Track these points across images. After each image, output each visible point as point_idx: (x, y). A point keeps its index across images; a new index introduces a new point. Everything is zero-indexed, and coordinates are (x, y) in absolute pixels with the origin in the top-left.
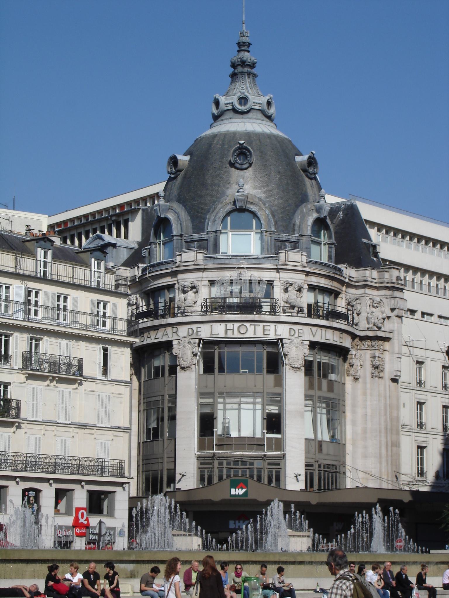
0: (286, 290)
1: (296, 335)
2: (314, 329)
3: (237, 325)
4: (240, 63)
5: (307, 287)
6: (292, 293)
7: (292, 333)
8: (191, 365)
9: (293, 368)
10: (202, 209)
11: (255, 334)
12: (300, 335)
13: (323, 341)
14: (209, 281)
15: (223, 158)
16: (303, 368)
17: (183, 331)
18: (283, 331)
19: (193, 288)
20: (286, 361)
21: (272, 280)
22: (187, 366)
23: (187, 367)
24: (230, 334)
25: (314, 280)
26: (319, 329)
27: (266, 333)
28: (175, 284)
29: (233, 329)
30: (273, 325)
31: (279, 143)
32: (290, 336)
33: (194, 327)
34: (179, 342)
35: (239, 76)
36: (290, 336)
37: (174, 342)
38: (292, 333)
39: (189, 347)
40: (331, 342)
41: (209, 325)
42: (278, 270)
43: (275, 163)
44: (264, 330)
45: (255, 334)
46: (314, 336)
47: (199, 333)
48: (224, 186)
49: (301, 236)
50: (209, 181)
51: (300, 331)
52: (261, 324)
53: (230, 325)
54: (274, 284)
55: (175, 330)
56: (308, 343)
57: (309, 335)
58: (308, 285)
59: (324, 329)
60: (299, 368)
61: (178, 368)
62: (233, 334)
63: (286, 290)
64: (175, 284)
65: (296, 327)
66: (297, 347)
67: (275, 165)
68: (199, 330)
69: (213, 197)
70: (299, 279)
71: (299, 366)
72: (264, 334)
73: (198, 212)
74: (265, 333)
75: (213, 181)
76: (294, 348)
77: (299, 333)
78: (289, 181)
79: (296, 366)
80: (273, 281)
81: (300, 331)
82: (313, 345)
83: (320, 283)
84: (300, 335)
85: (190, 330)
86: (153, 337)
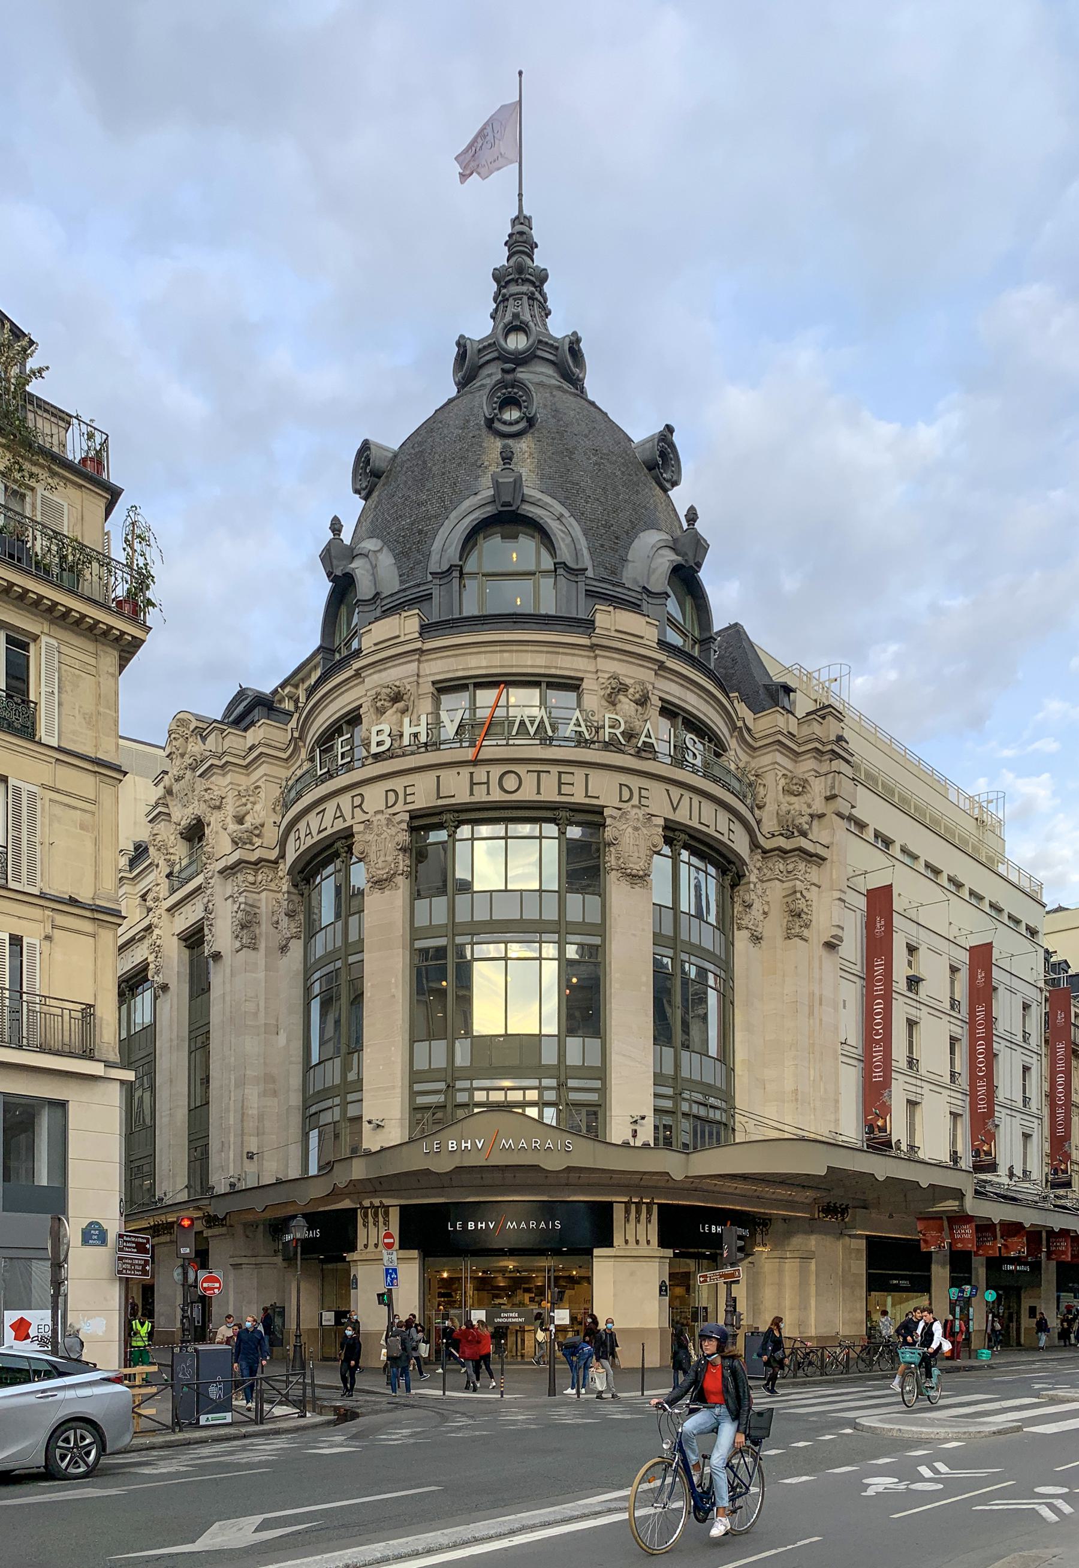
1: (635, 801)
6: (626, 705)
7: (626, 795)
12: (644, 801)
17: (374, 797)
19: (397, 698)
20: (611, 860)
21: (580, 675)
32: (621, 801)
33: (397, 784)
36: (621, 801)
38: (626, 797)
47: (409, 799)
54: (584, 685)
65: (635, 782)
66: (636, 829)
76: (630, 830)
77: (640, 797)
80: (582, 679)
84: (644, 801)
85: (391, 795)
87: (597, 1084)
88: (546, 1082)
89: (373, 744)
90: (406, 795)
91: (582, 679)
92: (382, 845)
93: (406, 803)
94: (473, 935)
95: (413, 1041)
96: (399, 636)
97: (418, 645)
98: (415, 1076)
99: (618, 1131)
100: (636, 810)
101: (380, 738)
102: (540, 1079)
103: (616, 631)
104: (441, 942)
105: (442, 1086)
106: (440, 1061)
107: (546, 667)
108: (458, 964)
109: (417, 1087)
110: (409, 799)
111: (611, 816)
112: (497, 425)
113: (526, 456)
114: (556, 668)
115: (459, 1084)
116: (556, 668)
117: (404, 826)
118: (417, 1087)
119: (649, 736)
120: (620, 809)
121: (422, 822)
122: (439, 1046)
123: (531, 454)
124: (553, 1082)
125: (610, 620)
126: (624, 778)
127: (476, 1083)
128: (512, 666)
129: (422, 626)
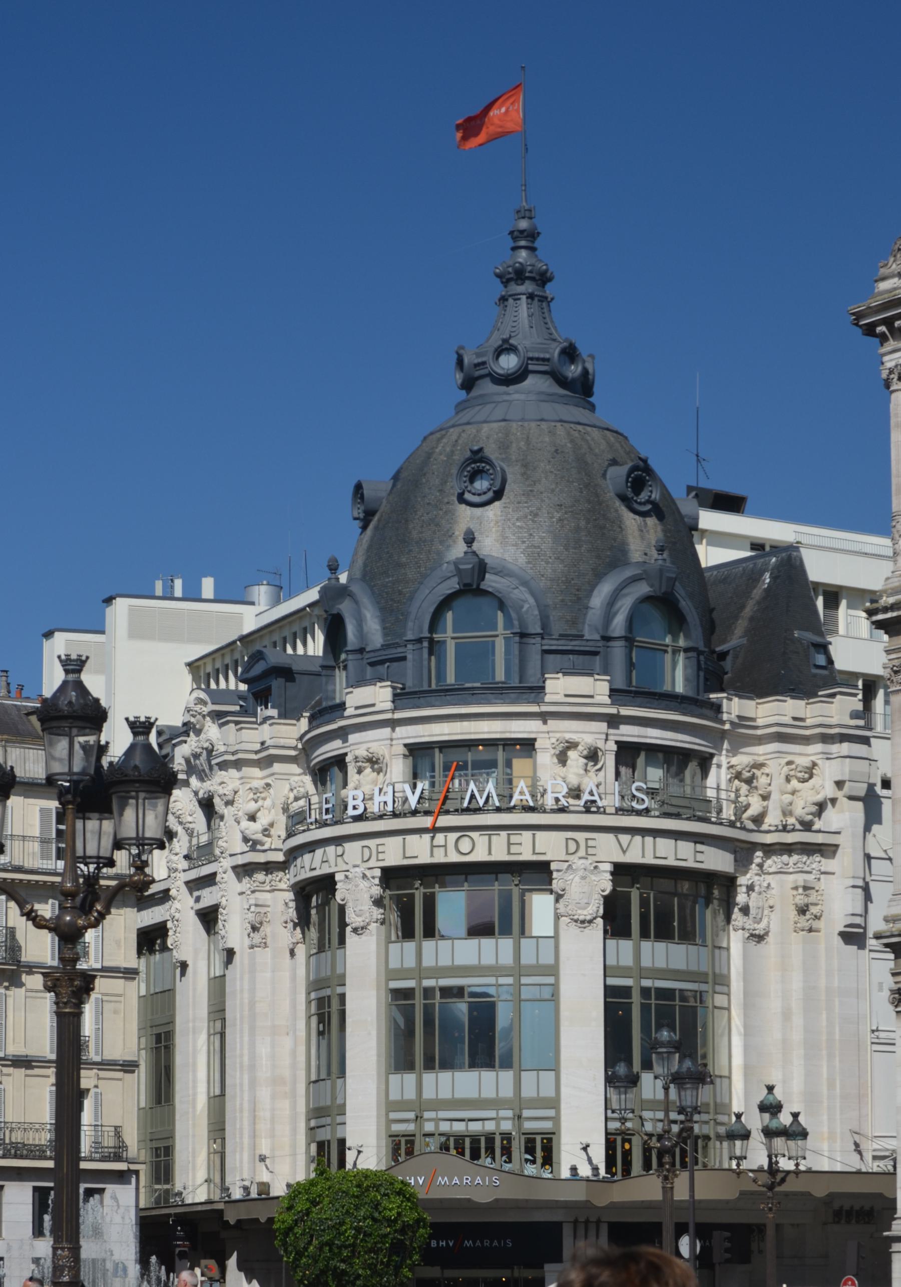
0: (562, 758)
1: (582, 853)
2: (625, 838)
3: (453, 836)
4: (512, 276)
5: (615, 748)
7: (572, 847)
8: (368, 924)
9: (576, 921)
10: (400, 593)
11: (490, 853)
12: (590, 851)
13: (649, 860)
14: (405, 745)
15: (446, 482)
16: (600, 921)
18: (549, 847)
21: (532, 736)
22: (362, 924)
23: (362, 928)
24: (439, 858)
25: (630, 733)
26: (638, 839)
27: (514, 849)
28: (346, 754)
29: (445, 846)
30: (527, 835)
31: (572, 441)
32: (567, 854)
33: (372, 843)
34: (347, 877)
35: (511, 301)
36: (567, 854)
37: (338, 877)
39: (363, 884)
40: (671, 862)
41: (399, 839)
42: (544, 717)
43: (553, 486)
44: (509, 844)
45: (490, 853)
46: (624, 852)
47: (381, 856)
48: (442, 542)
49: (607, 639)
50: (415, 534)
51: (590, 843)
52: (504, 834)
53: (440, 838)
54: (537, 745)
55: (340, 850)
56: (608, 867)
57: (610, 850)
58: (617, 742)
59: (649, 840)
60: (590, 922)
61: (348, 929)
62: (446, 855)
63: (562, 758)
64: (346, 754)
65: (581, 836)
67: (553, 491)
68: (381, 849)
69: (419, 567)
70: (590, 734)
71: (588, 918)
72: (509, 853)
73: (392, 600)
74: (512, 852)
75: (421, 533)
77: (587, 847)
78: (583, 523)
79: (582, 918)
80: (535, 740)
81: (590, 843)
82: (621, 871)
83: (646, 737)
84: (590, 851)
86: (307, 868)
87: (551, 1113)
88: (503, 1113)
89: (350, 808)
90: (378, 853)
91: (535, 740)
92: (359, 894)
93: (378, 860)
94: (437, 978)
95: (388, 1074)
96: (373, 705)
97: (388, 716)
98: (391, 1106)
99: (569, 1157)
100: (583, 861)
101: (355, 803)
102: (498, 1110)
103: (566, 696)
104: (411, 984)
105: (411, 1115)
106: (410, 1094)
107: (501, 732)
108: (425, 1005)
109: (393, 1116)
110: (381, 856)
111: (558, 871)
112: (467, 496)
113: (492, 524)
114: (510, 732)
115: (427, 1115)
116: (510, 732)
117: (377, 881)
118: (393, 1116)
119: (591, 793)
120: (567, 861)
121: (392, 876)
122: (410, 1078)
123: (497, 522)
124: (509, 1113)
125: (560, 687)
126: (570, 834)
127: (443, 1114)
128: (471, 733)
129: (395, 695)
